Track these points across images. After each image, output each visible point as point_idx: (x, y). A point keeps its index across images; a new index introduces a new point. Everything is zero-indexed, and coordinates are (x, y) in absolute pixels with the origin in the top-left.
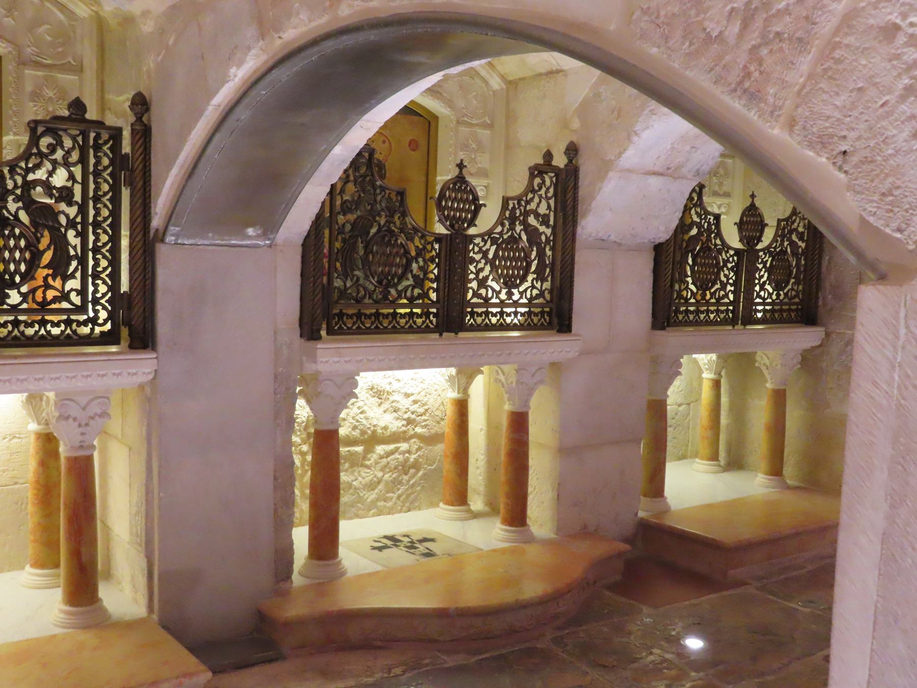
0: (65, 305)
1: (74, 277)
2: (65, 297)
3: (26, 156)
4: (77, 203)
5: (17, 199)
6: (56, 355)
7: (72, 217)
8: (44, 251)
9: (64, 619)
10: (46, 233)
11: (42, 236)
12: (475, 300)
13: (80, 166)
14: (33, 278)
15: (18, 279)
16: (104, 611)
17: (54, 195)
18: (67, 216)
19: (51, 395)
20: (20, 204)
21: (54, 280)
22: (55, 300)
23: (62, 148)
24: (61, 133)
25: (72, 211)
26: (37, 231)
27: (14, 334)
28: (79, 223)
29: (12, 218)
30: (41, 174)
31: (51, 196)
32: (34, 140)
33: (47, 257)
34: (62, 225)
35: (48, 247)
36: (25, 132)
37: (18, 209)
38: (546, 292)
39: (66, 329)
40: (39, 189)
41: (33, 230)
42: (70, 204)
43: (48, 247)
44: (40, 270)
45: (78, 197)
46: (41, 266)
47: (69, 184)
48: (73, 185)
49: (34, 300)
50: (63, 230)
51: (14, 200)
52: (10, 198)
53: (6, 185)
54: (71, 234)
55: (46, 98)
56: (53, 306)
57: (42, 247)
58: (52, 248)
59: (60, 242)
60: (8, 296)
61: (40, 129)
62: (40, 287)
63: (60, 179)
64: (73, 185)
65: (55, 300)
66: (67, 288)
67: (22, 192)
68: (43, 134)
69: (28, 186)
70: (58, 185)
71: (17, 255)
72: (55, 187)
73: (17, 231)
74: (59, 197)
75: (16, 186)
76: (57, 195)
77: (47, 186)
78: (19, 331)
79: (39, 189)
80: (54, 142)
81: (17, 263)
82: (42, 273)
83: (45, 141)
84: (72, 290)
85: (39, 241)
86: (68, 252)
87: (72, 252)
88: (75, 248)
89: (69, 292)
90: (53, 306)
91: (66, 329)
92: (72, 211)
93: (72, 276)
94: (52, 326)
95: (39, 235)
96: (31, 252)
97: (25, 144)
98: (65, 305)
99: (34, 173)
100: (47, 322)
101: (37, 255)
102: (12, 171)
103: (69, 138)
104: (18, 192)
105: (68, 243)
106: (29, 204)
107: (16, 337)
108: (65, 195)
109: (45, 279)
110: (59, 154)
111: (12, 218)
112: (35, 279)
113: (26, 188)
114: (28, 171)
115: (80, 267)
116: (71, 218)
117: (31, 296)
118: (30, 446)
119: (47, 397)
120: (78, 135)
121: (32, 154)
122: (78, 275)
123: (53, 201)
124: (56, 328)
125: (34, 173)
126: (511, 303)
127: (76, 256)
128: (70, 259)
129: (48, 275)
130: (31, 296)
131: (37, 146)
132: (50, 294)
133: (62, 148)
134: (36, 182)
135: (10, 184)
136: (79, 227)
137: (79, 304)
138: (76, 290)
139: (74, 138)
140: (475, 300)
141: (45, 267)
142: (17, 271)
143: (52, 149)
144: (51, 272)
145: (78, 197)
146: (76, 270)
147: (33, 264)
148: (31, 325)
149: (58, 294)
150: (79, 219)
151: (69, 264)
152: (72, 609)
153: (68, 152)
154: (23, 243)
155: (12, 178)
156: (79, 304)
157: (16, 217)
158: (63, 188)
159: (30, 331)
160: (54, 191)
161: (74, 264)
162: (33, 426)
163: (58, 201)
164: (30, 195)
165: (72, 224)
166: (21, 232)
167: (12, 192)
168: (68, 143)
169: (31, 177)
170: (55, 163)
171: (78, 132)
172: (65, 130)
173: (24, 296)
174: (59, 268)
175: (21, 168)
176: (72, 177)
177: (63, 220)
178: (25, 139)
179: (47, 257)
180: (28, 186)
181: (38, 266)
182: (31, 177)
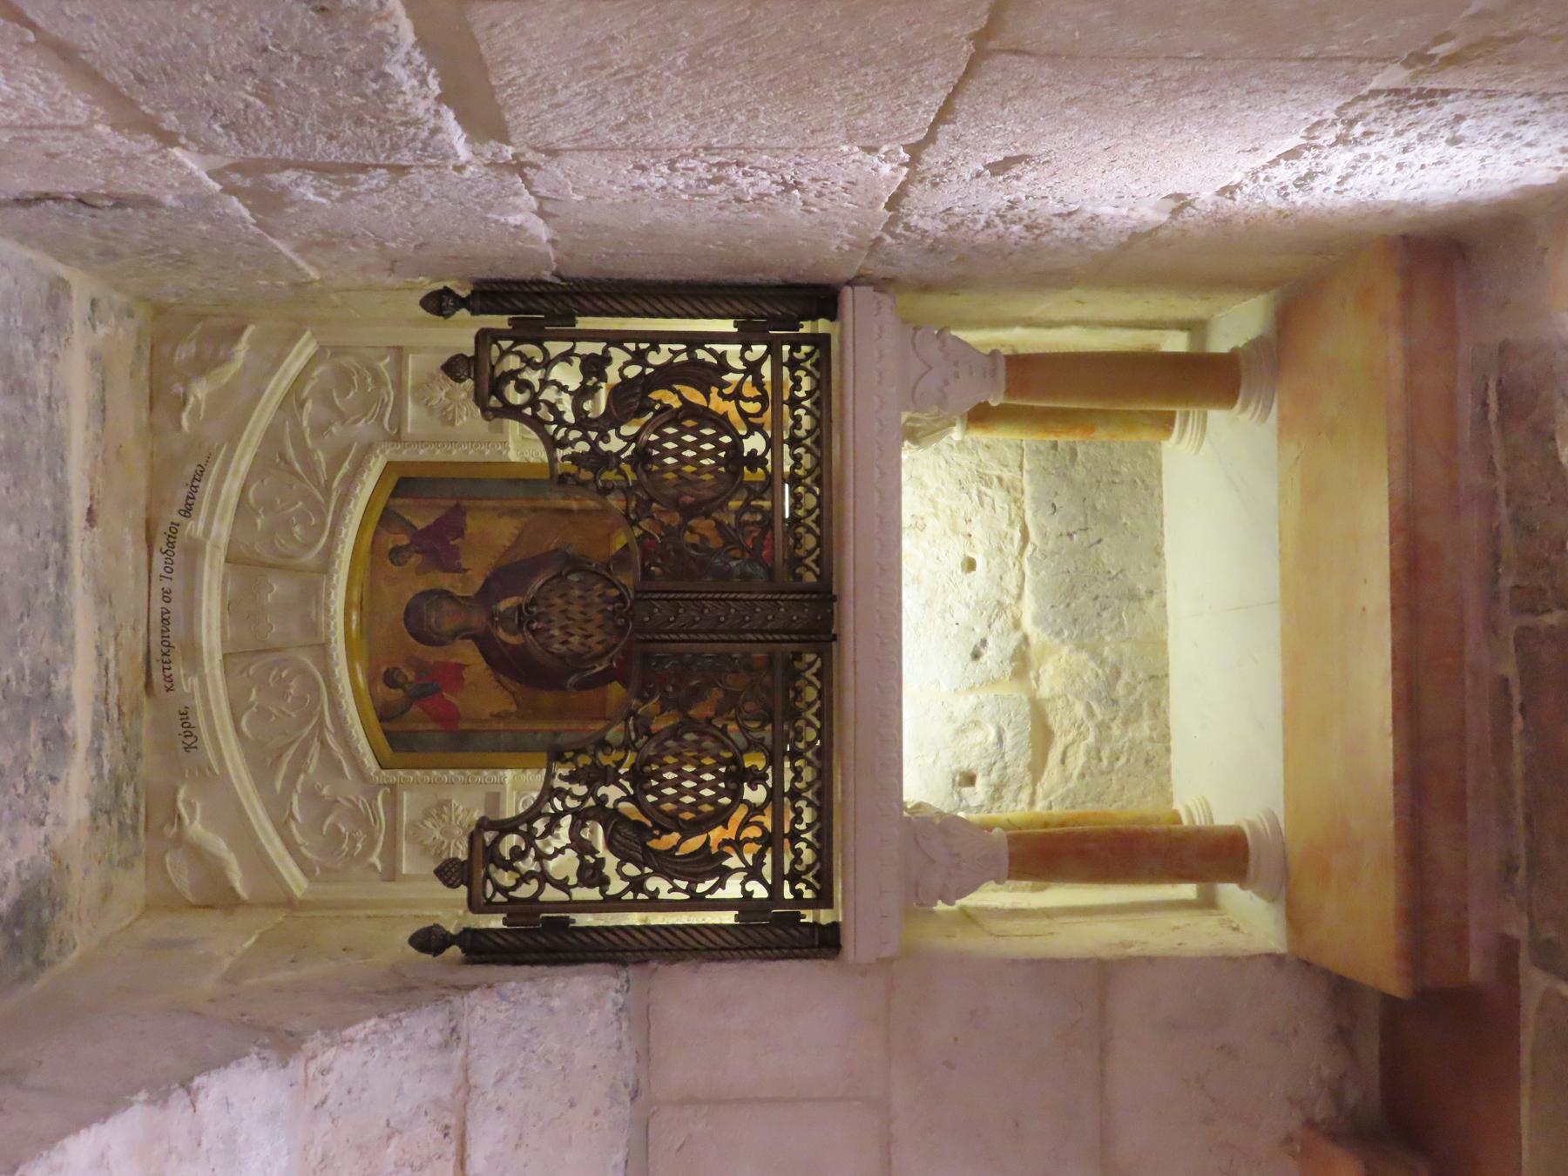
0: (766, 370)
1: (724, 354)
2: (753, 368)
3: (537, 424)
4: (605, 351)
5: (604, 437)
6: (842, 370)
7: (628, 357)
8: (681, 398)
9: (1258, 402)
10: (655, 395)
11: (660, 401)
12: (767, 871)
13: (547, 344)
14: (726, 414)
15: (726, 439)
16: (1254, 344)
17: (596, 383)
18: (626, 364)
19: (905, 416)
20: (612, 433)
21: (728, 384)
22: (758, 382)
23: (520, 371)
24: (498, 373)
25: (618, 356)
26: (652, 409)
27: (811, 880)
28: (637, 347)
29: (633, 445)
30: (566, 404)
31: (596, 388)
32: (514, 412)
33: (697, 398)
34: (642, 374)
35: (678, 393)
36: (501, 431)
37: (619, 436)
38: (749, 356)
39: (804, 369)
40: (587, 406)
41: (650, 415)
42: (606, 359)
43: (678, 393)
44: (712, 407)
45: (597, 348)
46: (705, 404)
47: (577, 361)
48: (577, 355)
49: (759, 415)
50: (649, 371)
51: (606, 442)
52: (603, 446)
53: (583, 453)
54: (656, 359)
55: (448, 401)
56: (768, 388)
57: (676, 404)
58: (677, 387)
59: (668, 376)
60: (753, 452)
61: (494, 401)
62: (738, 406)
63: (569, 375)
64: (577, 355)
65: (758, 382)
66: (739, 365)
67: (592, 430)
68: (502, 398)
69: (583, 422)
70: (581, 378)
71: (689, 438)
72: (583, 384)
73: (653, 437)
74: (597, 376)
75: (585, 438)
76: (594, 379)
77: (584, 393)
78: (806, 438)
79: (587, 406)
80: (513, 383)
81: (703, 439)
82: (718, 405)
83: (516, 398)
84: (742, 358)
85: (668, 407)
86: (683, 364)
87: (683, 357)
88: (676, 353)
89: (745, 362)
90: (768, 388)
91: (804, 369)
92: (618, 356)
93: (722, 357)
94: (799, 390)
95: (657, 407)
96: (685, 418)
97: (522, 431)
98: (766, 370)
99: (564, 412)
100: (793, 788)
101: (689, 409)
102: (563, 444)
103: (505, 360)
104: (593, 435)
105: (670, 362)
106: (613, 419)
107: (816, 836)
108: (594, 367)
109: (725, 398)
110: (534, 377)
111: (633, 445)
112: (726, 414)
113: (585, 424)
114: (560, 421)
115: (707, 346)
116: (628, 357)
117: (751, 419)
118: (981, 436)
119: (909, 420)
120: (499, 346)
121: (534, 416)
122: (719, 348)
123: (603, 384)
124: (803, 774)
125: (564, 412)
126: (773, 771)
127: (690, 351)
128: (694, 362)
129: (721, 394)
130: (751, 419)
131: (520, 408)
132: (749, 390)
133: (520, 371)
134: (577, 409)
135: (583, 447)
136: (643, 346)
137: (763, 348)
138: (743, 352)
139: (504, 353)
140: (767, 871)
141: (708, 399)
142: (713, 439)
143: (523, 386)
144: (714, 390)
145: (597, 348)
146: (711, 352)
147: (704, 416)
148: (797, 421)
149: (750, 378)
150: (631, 346)
151: (703, 363)
152: (1239, 401)
153: (529, 363)
154: (670, 430)
155: (572, 444)
156: (763, 348)
157: (629, 440)
158: (583, 368)
159: (806, 422)
160: (590, 383)
161: (701, 354)
162: (956, 434)
163: (603, 377)
164: (596, 420)
165: (639, 357)
166: (655, 433)
167: (594, 444)
168: (513, 363)
169: (569, 417)
170: (545, 383)
171: (494, 346)
172: (493, 368)
173: (752, 428)
174: (708, 376)
175: (556, 431)
176: (566, 357)
177: (633, 371)
178: (514, 427)
179: (697, 398)
180: (583, 422)
181: (707, 409)
182: (569, 417)
